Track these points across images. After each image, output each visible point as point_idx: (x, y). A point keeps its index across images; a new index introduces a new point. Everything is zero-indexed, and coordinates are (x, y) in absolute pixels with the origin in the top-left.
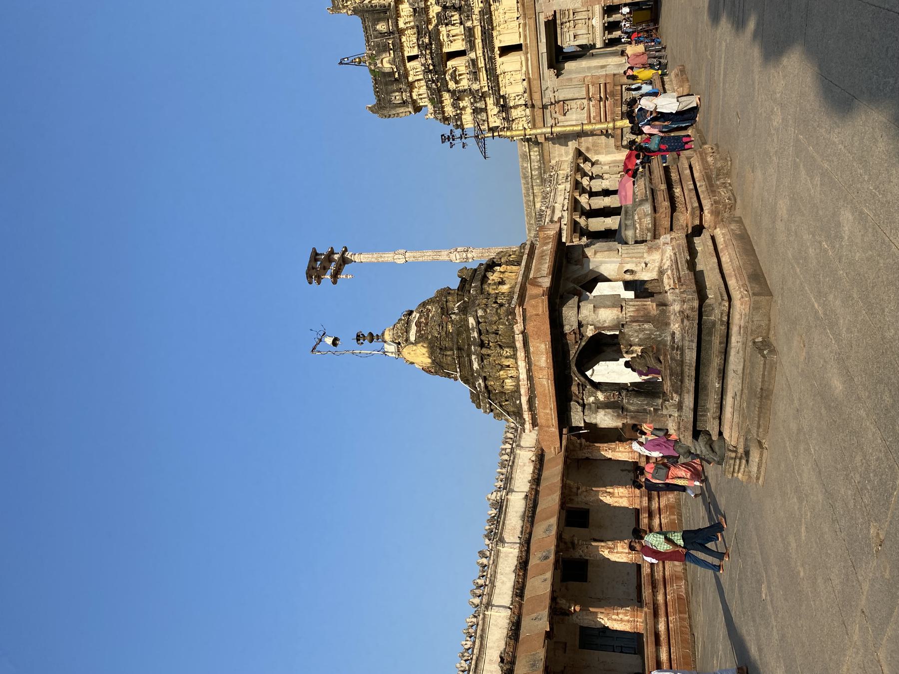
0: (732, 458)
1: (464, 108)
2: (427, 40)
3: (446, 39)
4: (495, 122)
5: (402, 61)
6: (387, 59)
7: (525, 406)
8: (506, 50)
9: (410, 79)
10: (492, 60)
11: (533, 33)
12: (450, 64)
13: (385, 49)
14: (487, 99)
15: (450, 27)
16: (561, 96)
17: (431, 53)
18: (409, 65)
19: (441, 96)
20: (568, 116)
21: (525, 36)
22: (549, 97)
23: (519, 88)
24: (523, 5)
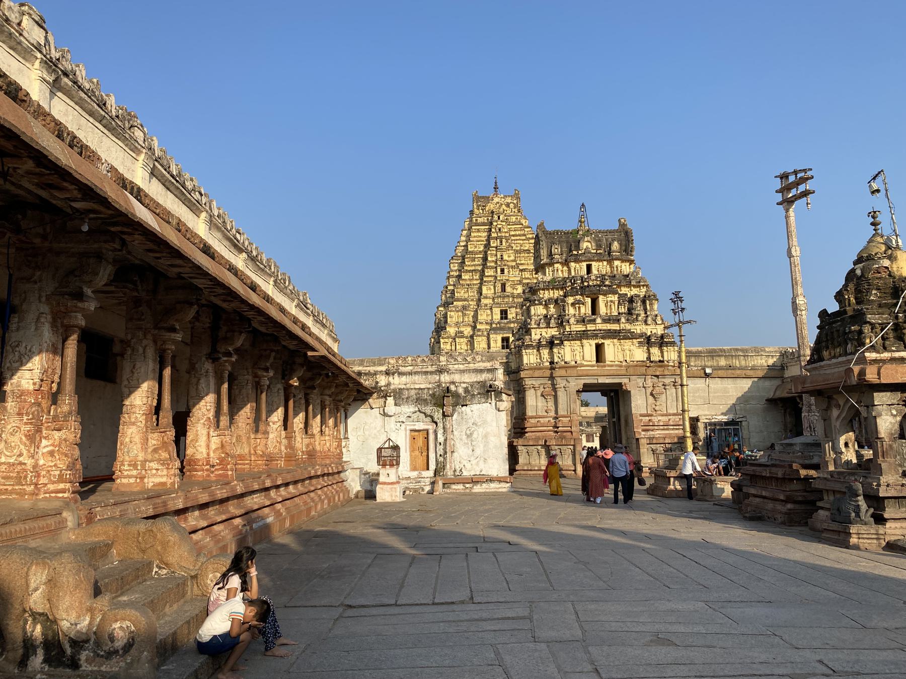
0: (877, 531)
1: (546, 306)
2: (607, 283)
3: (609, 299)
4: (536, 334)
5: (589, 258)
6: (590, 246)
7: (897, 355)
8: (599, 349)
9: (573, 264)
10: (595, 336)
11: (615, 373)
12: (589, 300)
13: (599, 246)
14: (556, 329)
15: (616, 303)
16: (561, 394)
17: (599, 286)
18: (584, 264)
19: (557, 289)
20: (540, 399)
21: (612, 366)
22: (561, 383)
23: (568, 359)
24: (636, 366)
